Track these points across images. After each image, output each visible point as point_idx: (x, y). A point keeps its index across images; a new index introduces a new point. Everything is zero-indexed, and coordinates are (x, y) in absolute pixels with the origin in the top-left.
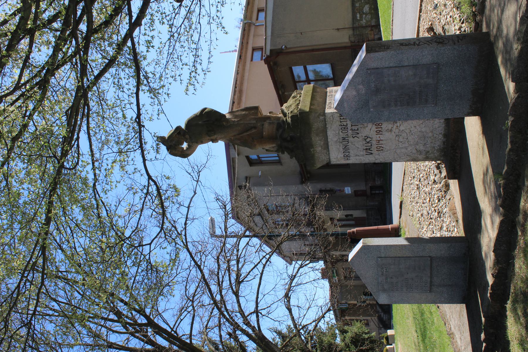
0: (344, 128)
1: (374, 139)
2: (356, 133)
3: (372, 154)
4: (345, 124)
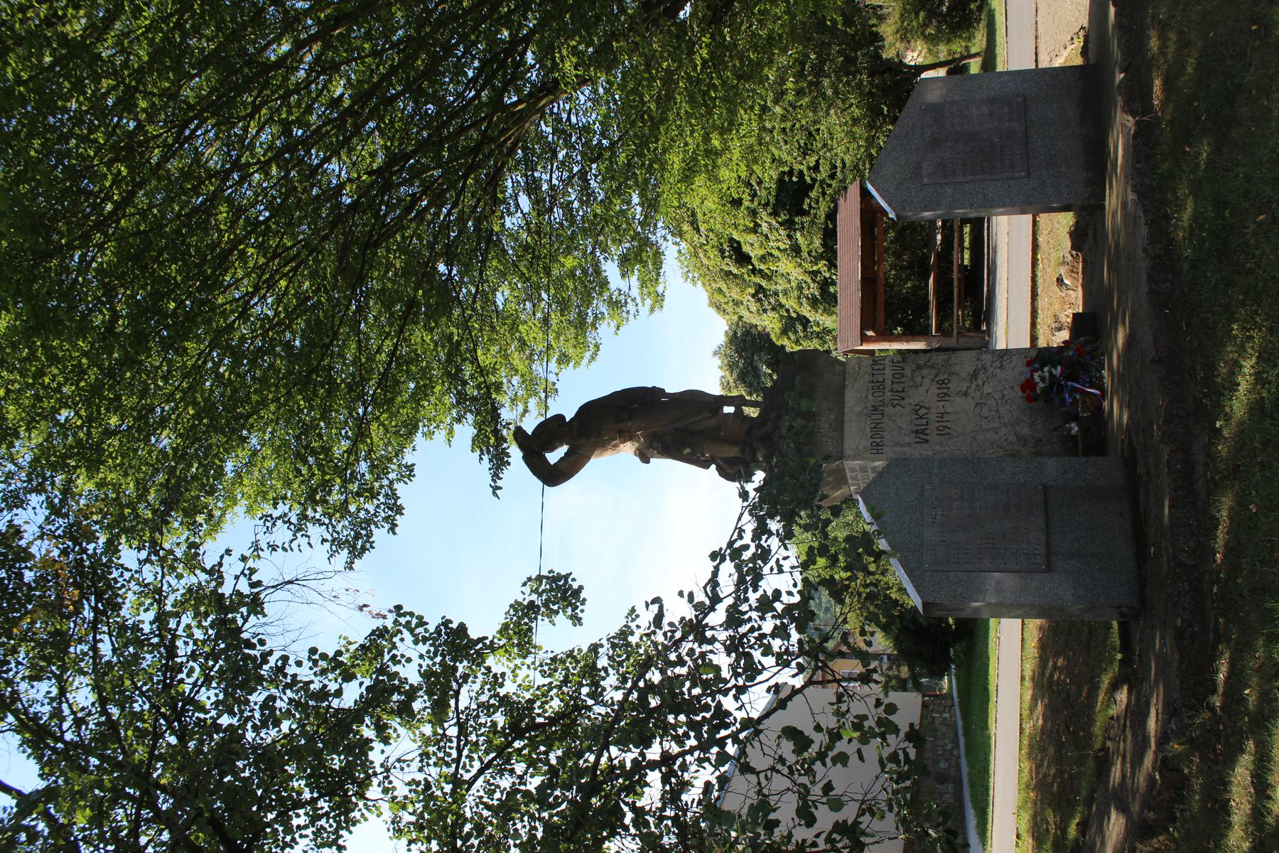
0: (878, 386)
1: (934, 410)
2: (900, 396)
3: (927, 441)
4: (881, 380)
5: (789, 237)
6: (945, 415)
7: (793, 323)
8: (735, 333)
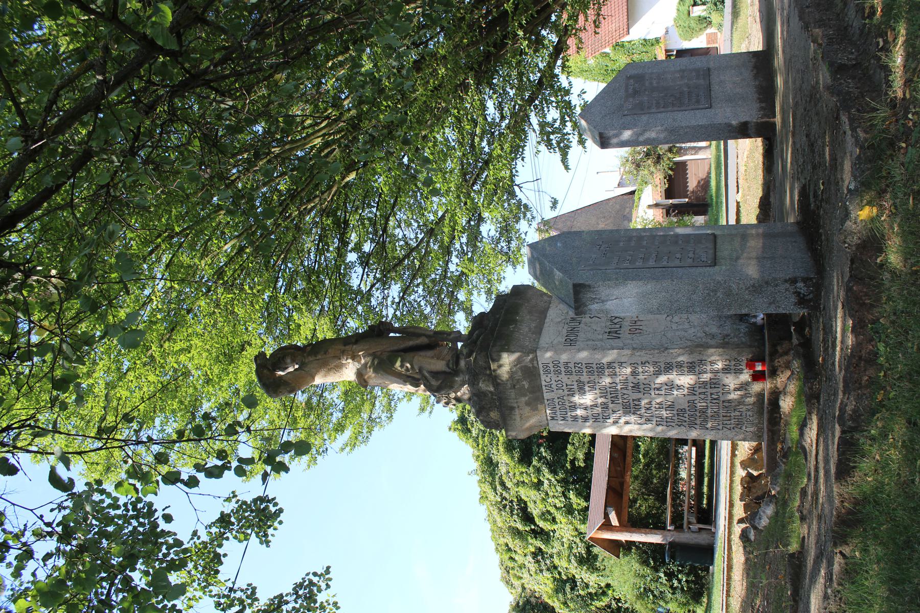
3: (619, 338)
6: (639, 323)
8: (518, 603)
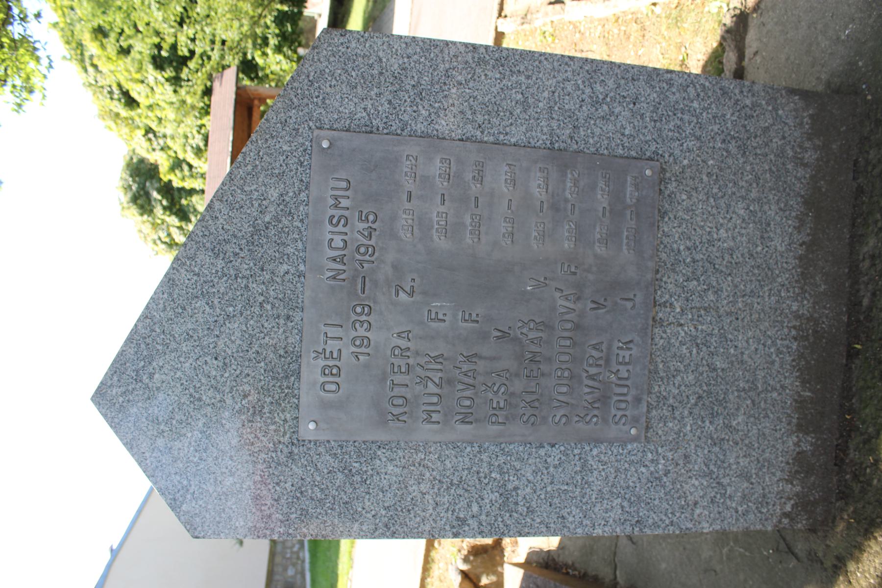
5: (175, 91)
7: (177, 164)
8: (132, 159)
